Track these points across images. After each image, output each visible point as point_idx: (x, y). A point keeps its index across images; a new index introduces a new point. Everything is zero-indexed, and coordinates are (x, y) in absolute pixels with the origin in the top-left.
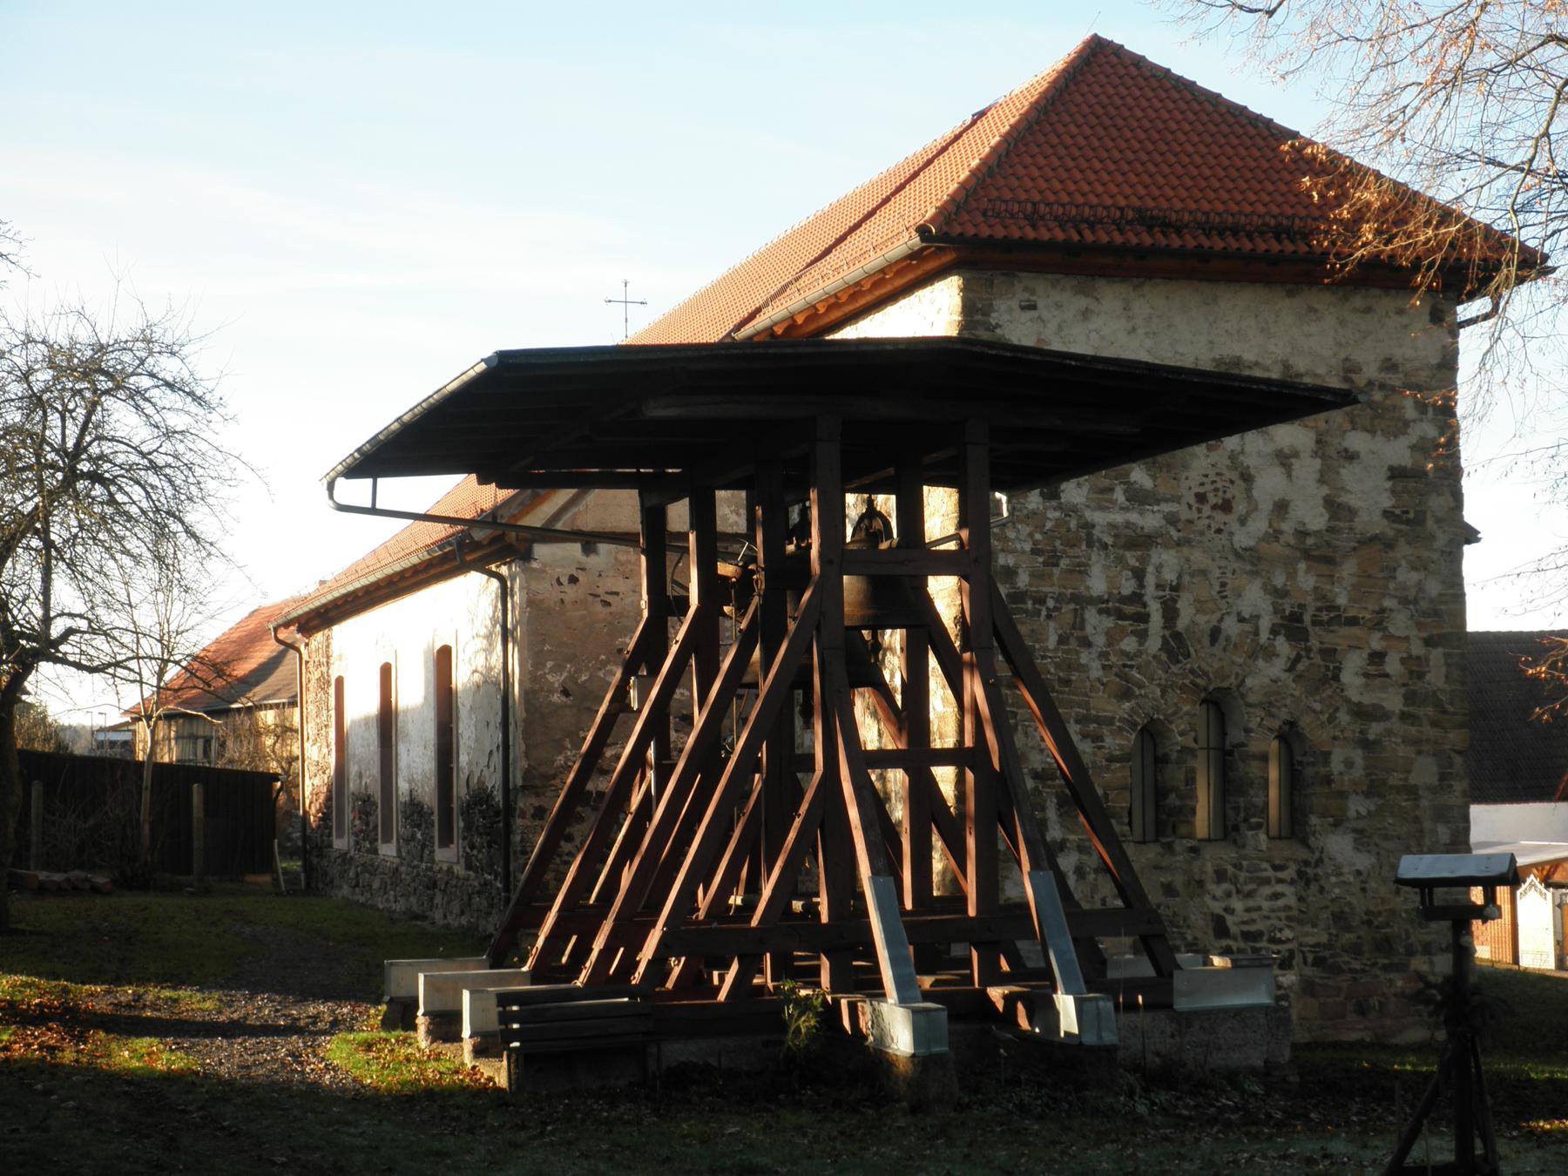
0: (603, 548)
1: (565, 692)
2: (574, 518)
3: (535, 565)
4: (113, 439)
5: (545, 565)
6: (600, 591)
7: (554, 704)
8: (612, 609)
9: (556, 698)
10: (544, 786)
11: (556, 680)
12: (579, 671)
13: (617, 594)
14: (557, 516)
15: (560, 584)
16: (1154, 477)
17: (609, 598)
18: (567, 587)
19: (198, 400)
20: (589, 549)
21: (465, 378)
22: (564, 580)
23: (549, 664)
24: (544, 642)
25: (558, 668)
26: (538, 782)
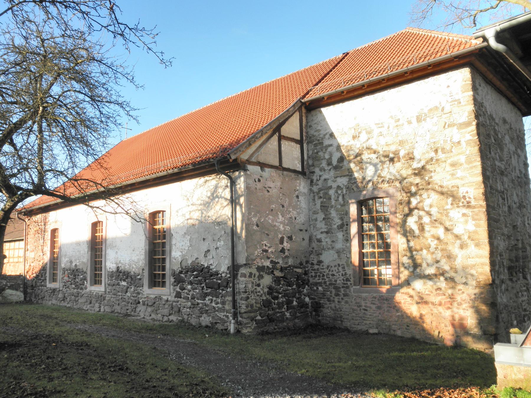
0: (267, 170)
1: (257, 226)
2: (258, 157)
3: (248, 173)
4: (81, 179)
5: (251, 173)
6: (266, 186)
7: (253, 230)
8: (269, 194)
9: (255, 227)
10: (252, 264)
11: (255, 220)
12: (261, 217)
13: (270, 188)
14: (252, 155)
15: (256, 181)
16: (503, 137)
17: (269, 189)
18: (257, 183)
19: (522, 345)
20: (262, 169)
21: (514, 22)
22: (257, 180)
23: (253, 213)
24: (251, 204)
25: (255, 216)
26: (250, 262)
